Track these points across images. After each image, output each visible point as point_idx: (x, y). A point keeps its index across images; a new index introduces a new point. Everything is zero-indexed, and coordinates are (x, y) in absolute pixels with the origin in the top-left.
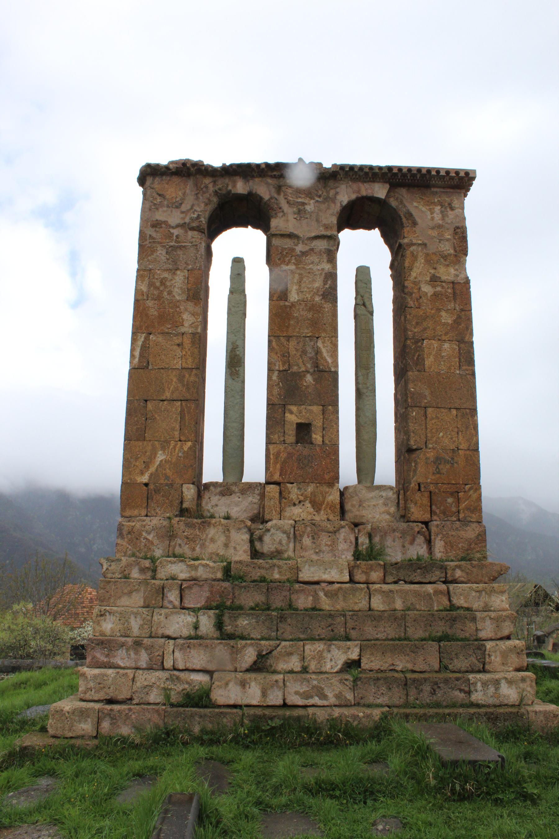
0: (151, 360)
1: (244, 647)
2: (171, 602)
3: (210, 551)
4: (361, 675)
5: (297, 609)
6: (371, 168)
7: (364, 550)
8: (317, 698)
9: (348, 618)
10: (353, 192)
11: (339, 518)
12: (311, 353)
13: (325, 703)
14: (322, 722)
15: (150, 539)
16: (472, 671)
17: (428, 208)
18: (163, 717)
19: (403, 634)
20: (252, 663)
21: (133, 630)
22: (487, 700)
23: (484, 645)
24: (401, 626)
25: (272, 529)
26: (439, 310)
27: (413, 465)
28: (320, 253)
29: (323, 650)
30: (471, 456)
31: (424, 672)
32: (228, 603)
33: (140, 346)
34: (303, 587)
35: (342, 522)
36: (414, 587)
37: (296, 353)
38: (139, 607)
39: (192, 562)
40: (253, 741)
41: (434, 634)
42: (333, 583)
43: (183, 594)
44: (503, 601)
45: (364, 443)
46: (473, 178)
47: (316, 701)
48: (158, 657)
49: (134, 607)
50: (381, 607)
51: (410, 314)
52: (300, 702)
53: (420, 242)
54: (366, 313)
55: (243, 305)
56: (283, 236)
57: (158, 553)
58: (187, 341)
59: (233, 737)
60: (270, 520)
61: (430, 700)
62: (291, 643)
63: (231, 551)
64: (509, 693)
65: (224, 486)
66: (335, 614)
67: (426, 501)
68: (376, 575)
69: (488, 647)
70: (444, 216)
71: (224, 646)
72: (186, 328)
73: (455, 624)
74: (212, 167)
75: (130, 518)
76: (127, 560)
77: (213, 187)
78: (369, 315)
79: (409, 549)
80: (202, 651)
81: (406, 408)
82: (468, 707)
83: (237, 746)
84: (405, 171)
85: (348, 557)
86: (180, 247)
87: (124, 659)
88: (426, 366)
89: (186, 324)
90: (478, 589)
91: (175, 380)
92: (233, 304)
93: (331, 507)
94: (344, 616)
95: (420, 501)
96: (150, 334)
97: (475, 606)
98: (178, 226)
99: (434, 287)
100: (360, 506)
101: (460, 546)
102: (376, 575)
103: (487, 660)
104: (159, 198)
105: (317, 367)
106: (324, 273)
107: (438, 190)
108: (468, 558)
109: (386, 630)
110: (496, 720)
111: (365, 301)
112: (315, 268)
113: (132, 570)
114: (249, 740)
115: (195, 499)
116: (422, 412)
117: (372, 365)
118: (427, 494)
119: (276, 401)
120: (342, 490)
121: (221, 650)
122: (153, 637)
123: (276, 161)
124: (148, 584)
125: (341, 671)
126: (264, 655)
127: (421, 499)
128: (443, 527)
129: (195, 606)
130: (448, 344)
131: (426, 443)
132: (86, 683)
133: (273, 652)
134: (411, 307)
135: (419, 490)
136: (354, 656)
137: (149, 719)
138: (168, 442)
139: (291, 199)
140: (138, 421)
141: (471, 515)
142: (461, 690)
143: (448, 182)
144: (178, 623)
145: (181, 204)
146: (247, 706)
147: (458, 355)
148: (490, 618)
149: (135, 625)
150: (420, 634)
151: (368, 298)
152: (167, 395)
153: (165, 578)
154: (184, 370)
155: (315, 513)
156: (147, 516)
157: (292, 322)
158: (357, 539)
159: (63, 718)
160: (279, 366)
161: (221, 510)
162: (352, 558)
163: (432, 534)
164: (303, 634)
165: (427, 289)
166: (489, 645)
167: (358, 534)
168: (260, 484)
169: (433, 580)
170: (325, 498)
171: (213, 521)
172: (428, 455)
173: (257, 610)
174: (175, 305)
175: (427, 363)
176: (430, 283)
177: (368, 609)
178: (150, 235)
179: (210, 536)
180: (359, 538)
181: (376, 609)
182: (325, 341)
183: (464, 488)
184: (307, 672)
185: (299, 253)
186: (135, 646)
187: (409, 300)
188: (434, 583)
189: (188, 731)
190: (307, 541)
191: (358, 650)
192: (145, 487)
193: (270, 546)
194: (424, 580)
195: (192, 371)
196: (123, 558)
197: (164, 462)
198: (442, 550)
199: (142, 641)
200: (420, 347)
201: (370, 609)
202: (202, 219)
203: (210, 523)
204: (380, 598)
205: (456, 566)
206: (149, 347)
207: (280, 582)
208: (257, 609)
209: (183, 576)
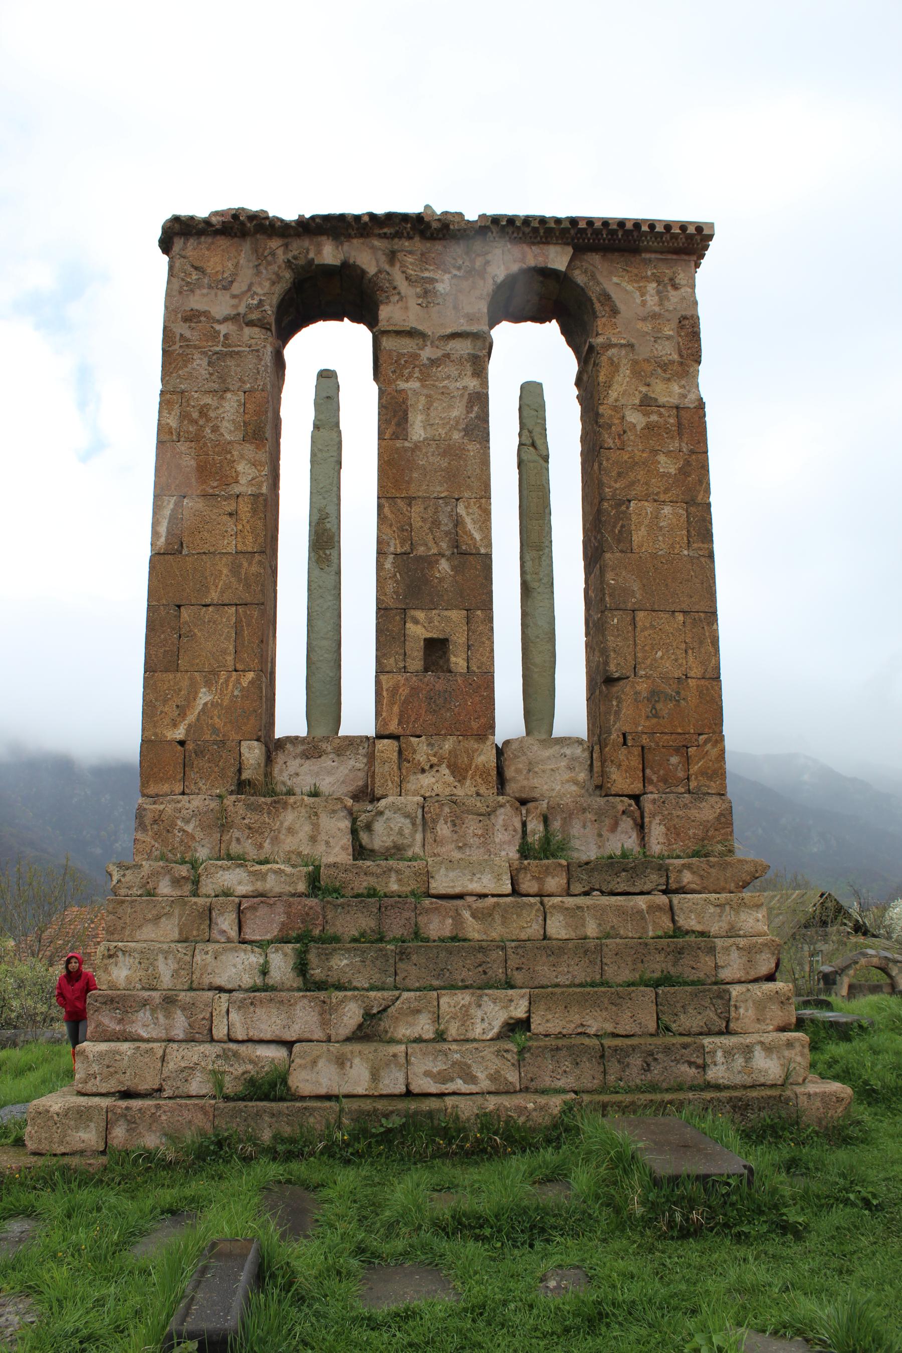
1: (342, 1001)
3: (288, 849)
4: (530, 1043)
5: (427, 940)
6: (543, 220)
7: (537, 843)
8: (460, 1081)
9: (510, 951)
10: (515, 261)
11: (495, 791)
12: (447, 524)
13: (473, 1088)
14: (468, 1120)
15: (190, 831)
16: (709, 1033)
17: (636, 285)
18: (211, 1118)
19: (598, 977)
20: (355, 1028)
21: (162, 978)
22: (731, 1077)
23: (728, 992)
24: (595, 964)
25: (387, 812)
26: (655, 452)
27: (615, 703)
28: (460, 361)
29: (470, 1004)
30: (707, 689)
31: (633, 1035)
32: (316, 932)
33: (168, 517)
34: (436, 903)
35: (500, 798)
36: (616, 901)
37: (423, 524)
38: (172, 941)
39: (258, 867)
40: (358, 1151)
41: (648, 975)
42: (485, 896)
43: (243, 920)
44: (758, 921)
45: (536, 670)
46: (710, 237)
47: (459, 1086)
48: (203, 1022)
49: (164, 942)
50: (563, 934)
51: (608, 459)
52: (433, 1088)
53: (623, 342)
54: (538, 458)
55: (336, 448)
56: (398, 333)
57: (202, 853)
58: (244, 508)
59: (325, 1147)
60: (384, 797)
61: (642, 1080)
62: (418, 993)
63: (322, 848)
64: (767, 1066)
65: (309, 743)
66: (489, 946)
67: (636, 762)
68: (554, 883)
69: (734, 993)
70: (662, 298)
71: (310, 1002)
72: (243, 487)
73: (681, 958)
74: (282, 221)
75: (155, 798)
76: (150, 866)
77: (284, 253)
78: (542, 462)
79: (608, 840)
80: (274, 1010)
81: (602, 612)
82: (702, 1090)
83: (331, 1160)
84: (598, 225)
85: (511, 855)
86: (232, 354)
87: (148, 1026)
88: (635, 547)
89: (243, 480)
90: (718, 902)
91: (225, 571)
92: (320, 447)
93: (483, 773)
94: (504, 948)
95: (626, 763)
96: (184, 497)
97: (714, 929)
98: (226, 319)
99: (647, 414)
100: (529, 770)
101: (691, 832)
102: (554, 883)
103: (733, 1014)
105: (457, 547)
106: (466, 394)
107: (653, 256)
108: (703, 852)
109: (571, 970)
110: (746, 1109)
111: (535, 438)
112: (453, 386)
113: (159, 881)
114: (350, 1150)
115: (262, 765)
117: (547, 543)
118: (637, 751)
119: (391, 603)
120: (500, 746)
121: (304, 1008)
122: (195, 990)
123: (387, 211)
124: (185, 903)
125: (498, 1037)
126: (374, 1014)
127: (628, 759)
128: (664, 802)
129: (263, 938)
130: (669, 507)
131: (635, 668)
132: (85, 1065)
133: (389, 1010)
134: (610, 449)
135: (625, 743)
136: (520, 1012)
137: (190, 1122)
138: (214, 673)
139: (412, 273)
140: (166, 639)
141: (707, 783)
142: (690, 1064)
143: (668, 243)
144: (235, 966)
145: (232, 282)
146: (346, 1096)
147: (685, 525)
148: (738, 948)
149: (165, 970)
150: (626, 975)
151: (541, 434)
152: (214, 596)
153: (213, 894)
154: (241, 556)
155: (456, 784)
156: (183, 793)
157: (415, 475)
158: (524, 824)
159: (50, 1123)
160: (395, 546)
161: (305, 782)
162: (517, 856)
163: (646, 815)
164: (438, 979)
165: (635, 418)
166: (736, 991)
167: (526, 817)
168: (367, 738)
169: (646, 888)
170: (472, 760)
171: (292, 799)
172: (638, 688)
173: (364, 943)
174: (225, 448)
176: (639, 408)
177: (541, 938)
178: (181, 335)
179: (286, 824)
180: (528, 823)
181: (554, 936)
182: (469, 504)
183: (697, 740)
184: (445, 1040)
185: (425, 361)
186: (166, 1005)
187: (607, 436)
188: (649, 893)
189: (253, 1139)
190: (443, 829)
191: (527, 1003)
192: (179, 747)
193: (385, 838)
194: (632, 890)
195: (253, 557)
196: (144, 863)
197: (209, 705)
198: (662, 840)
199: (176, 995)
200: (624, 512)
201: (545, 937)
202: (267, 307)
203: (286, 803)
204: (562, 918)
205: (683, 865)
206: (182, 519)
207: (400, 896)
208: (363, 940)
209: (242, 890)
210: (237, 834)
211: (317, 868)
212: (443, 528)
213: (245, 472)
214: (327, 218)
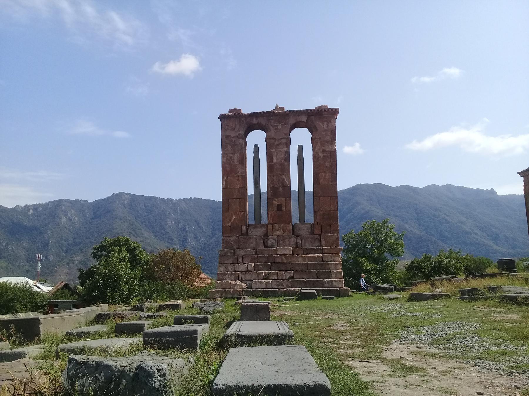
6: (300, 111)
26: (325, 162)
52: (276, 288)
53: (318, 137)
58: (240, 178)
60: (270, 236)
70: (328, 125)
75: (226, 237)
84: (313, 111)
91: (237, 192)
98: (234, 137)
99: (323, 153)
104: (227, 126)
112: (282, 150)
118: (320, 226)
135: (318, 224)
136: (292, 275)
142: (322, 284)
145: (235, 129)
152: (235, 197)
156: (231, 236)
163: (321, 238)
165: (321, 155)
169: (319, 253)
178: (225, 141)
179: (251, 242)
185: (276, 144)
192: (230, 227)
194: (315, 253)
209: (243, 254)
210: (241, 244)
211: (257, 250)
213: (240, 171)
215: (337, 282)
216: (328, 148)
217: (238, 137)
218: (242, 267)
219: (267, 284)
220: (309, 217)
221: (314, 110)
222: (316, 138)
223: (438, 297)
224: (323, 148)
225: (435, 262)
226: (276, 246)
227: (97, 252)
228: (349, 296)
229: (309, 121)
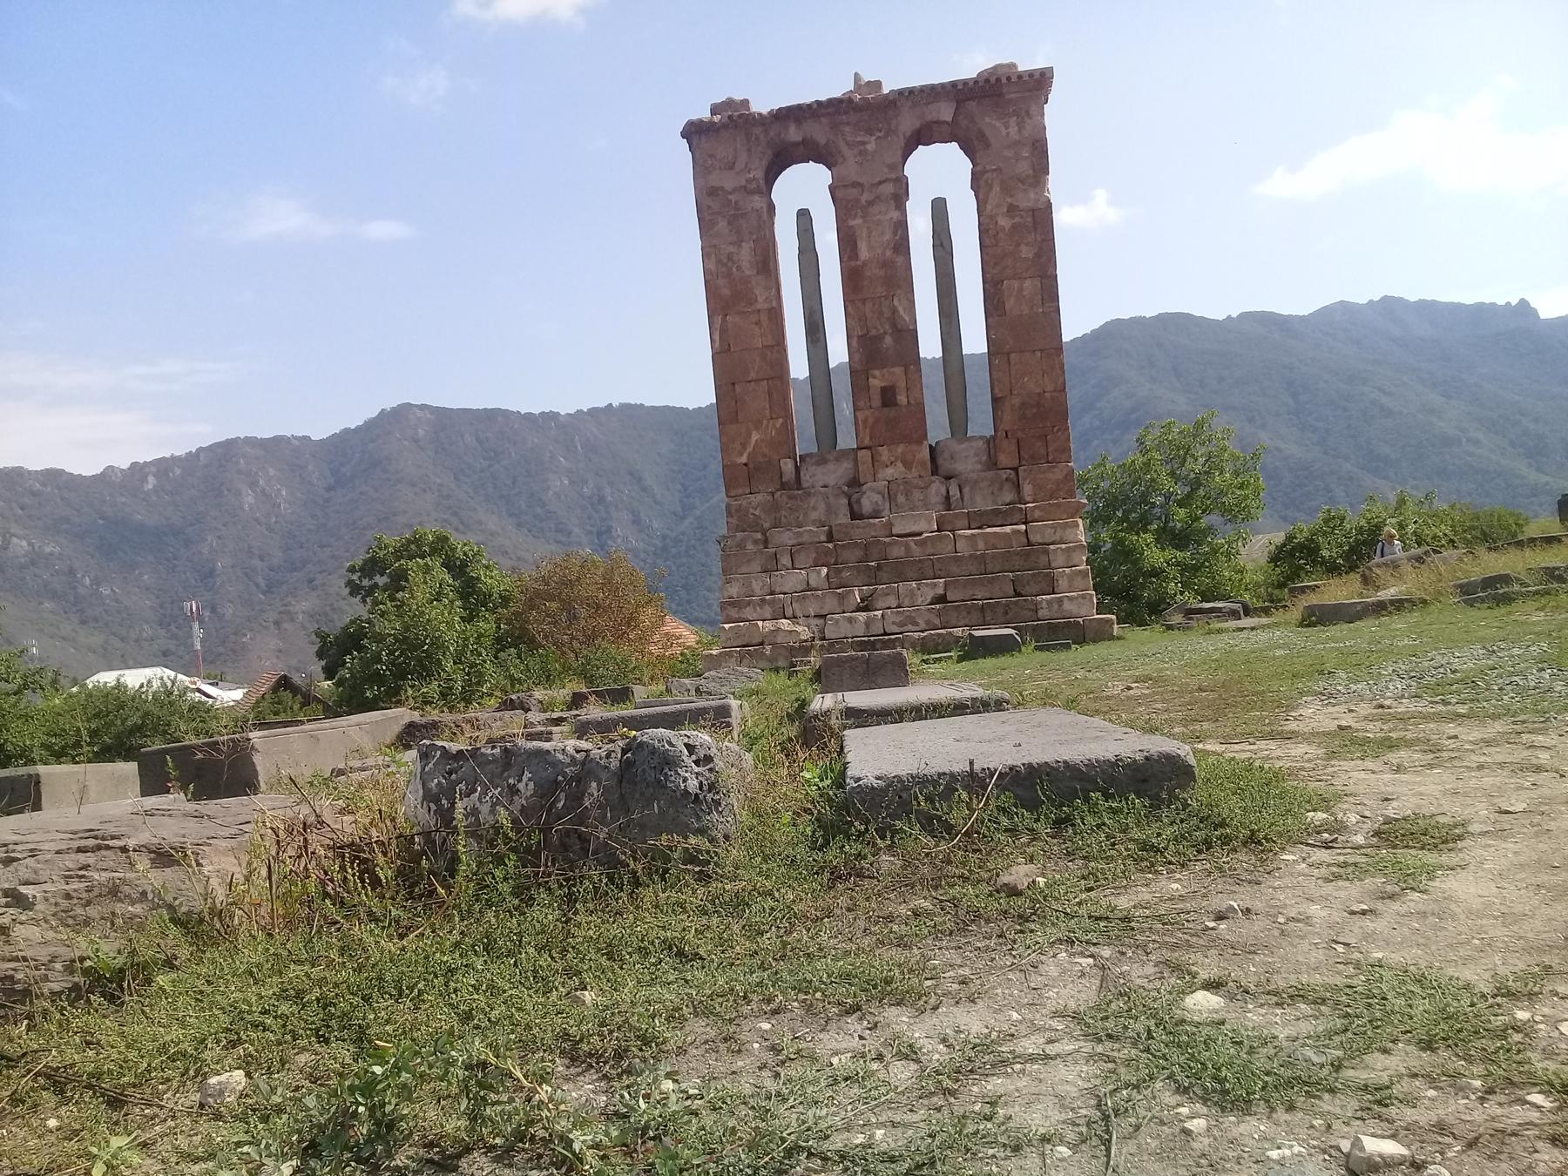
0: (731, 342)
2: (784, 565)
6: (932, 88)
26: (1018, 245)
58: (764, 318)
67: (1014, 448)
89: (760, 300)
91: (758, 359)
93: (923, 463)
98: (734, 190)
99: (1013, 218)
107: (1013, 96)
116: (1006, 359)
118: (1015, 441)
119: (858, 367)
124: (762, 553)
136: (941, 591)
142: (1030, 610)
145: (734, 163)
152: (753, 375)
165: (1004, 222)
169: (1015, 521)
175: (1007, 307)
179: (811, 505)
209: (791, 542)
210: (784, 513)
211: (830, 527)
212: (886, 315)
213: (760, 295)
214: (789, 109)
215: (1075, 602)
216: (1025, 200)
217: (746, 190)
218: (792, 580)
219: (868, 624)
220: (981, 422)
221: (976, 81)
222: (986, 172)
223: (1391, 608)
224: (1009, 200)
225: (1360, 530)
226: (887, 512)
227: (360, 578)
228: (1112, 638)
229: (961, 117)
